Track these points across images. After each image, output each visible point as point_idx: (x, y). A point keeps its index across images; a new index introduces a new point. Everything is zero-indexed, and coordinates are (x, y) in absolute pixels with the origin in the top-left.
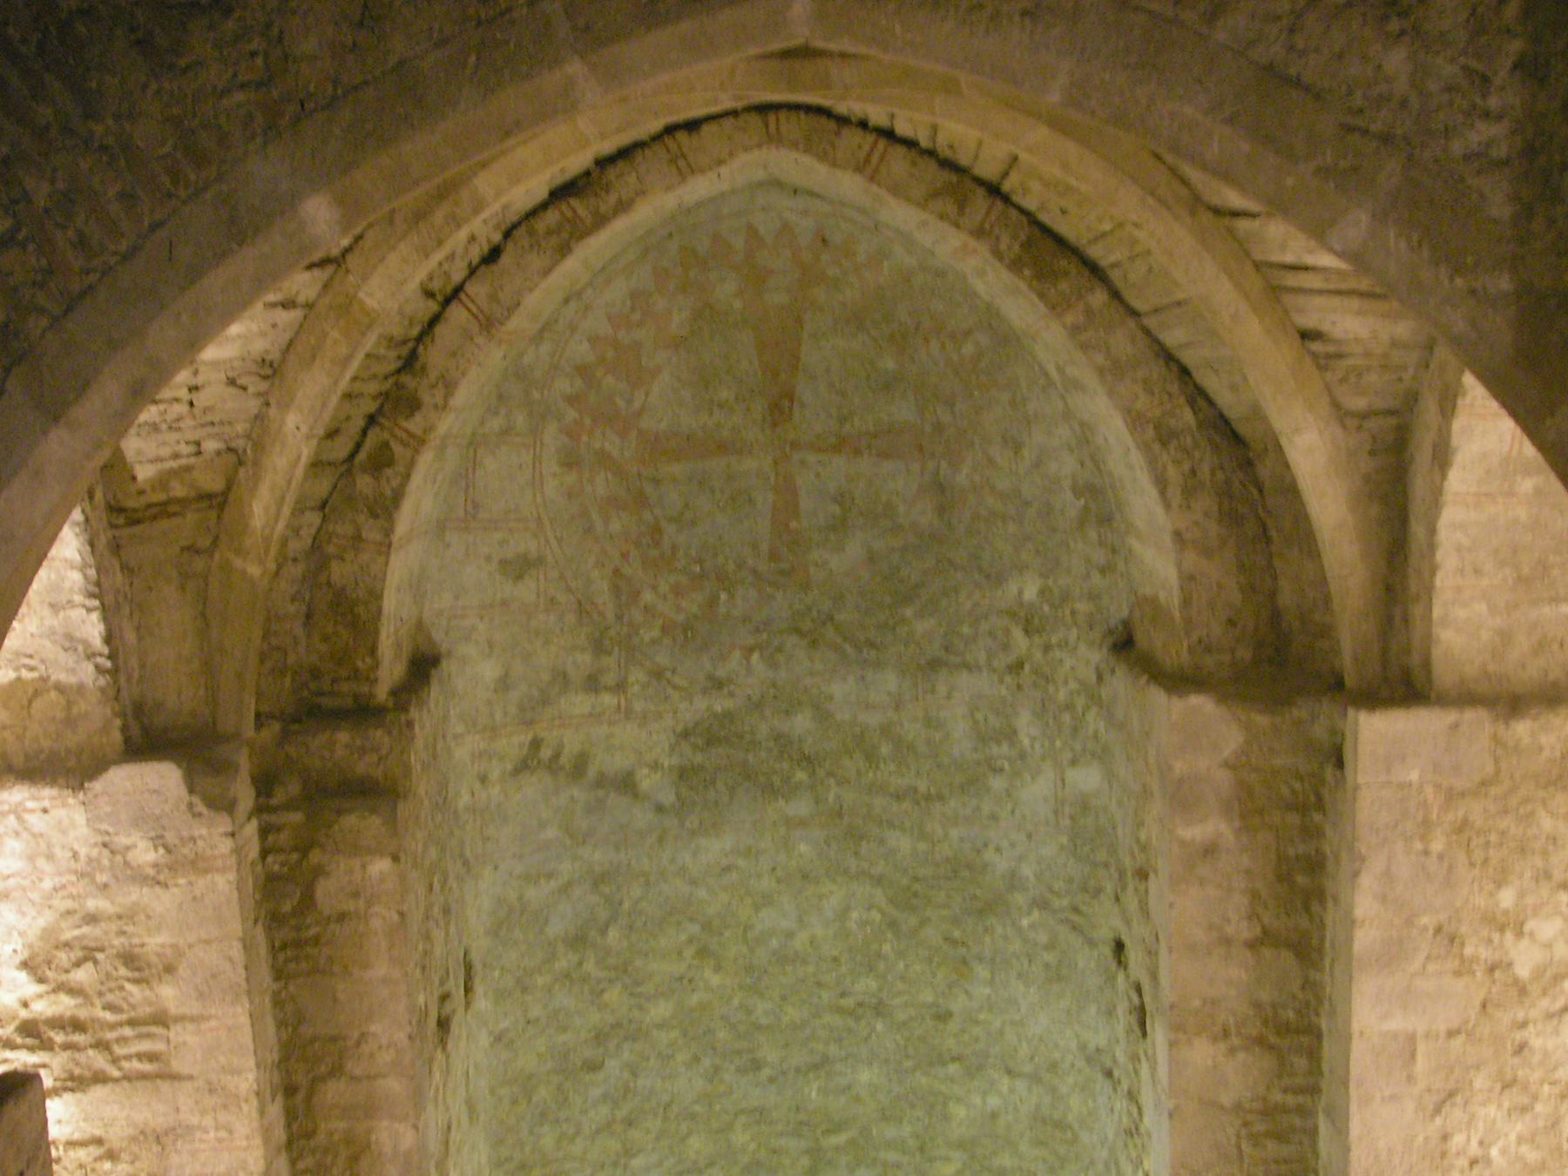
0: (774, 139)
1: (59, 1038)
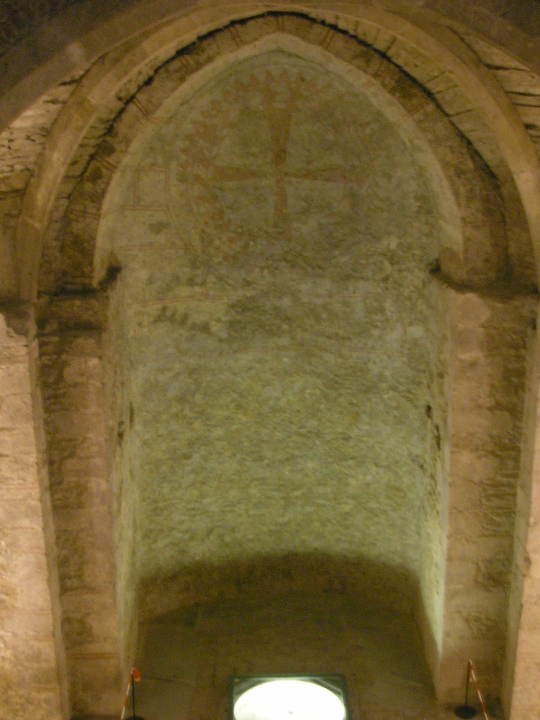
0: (282, 29)
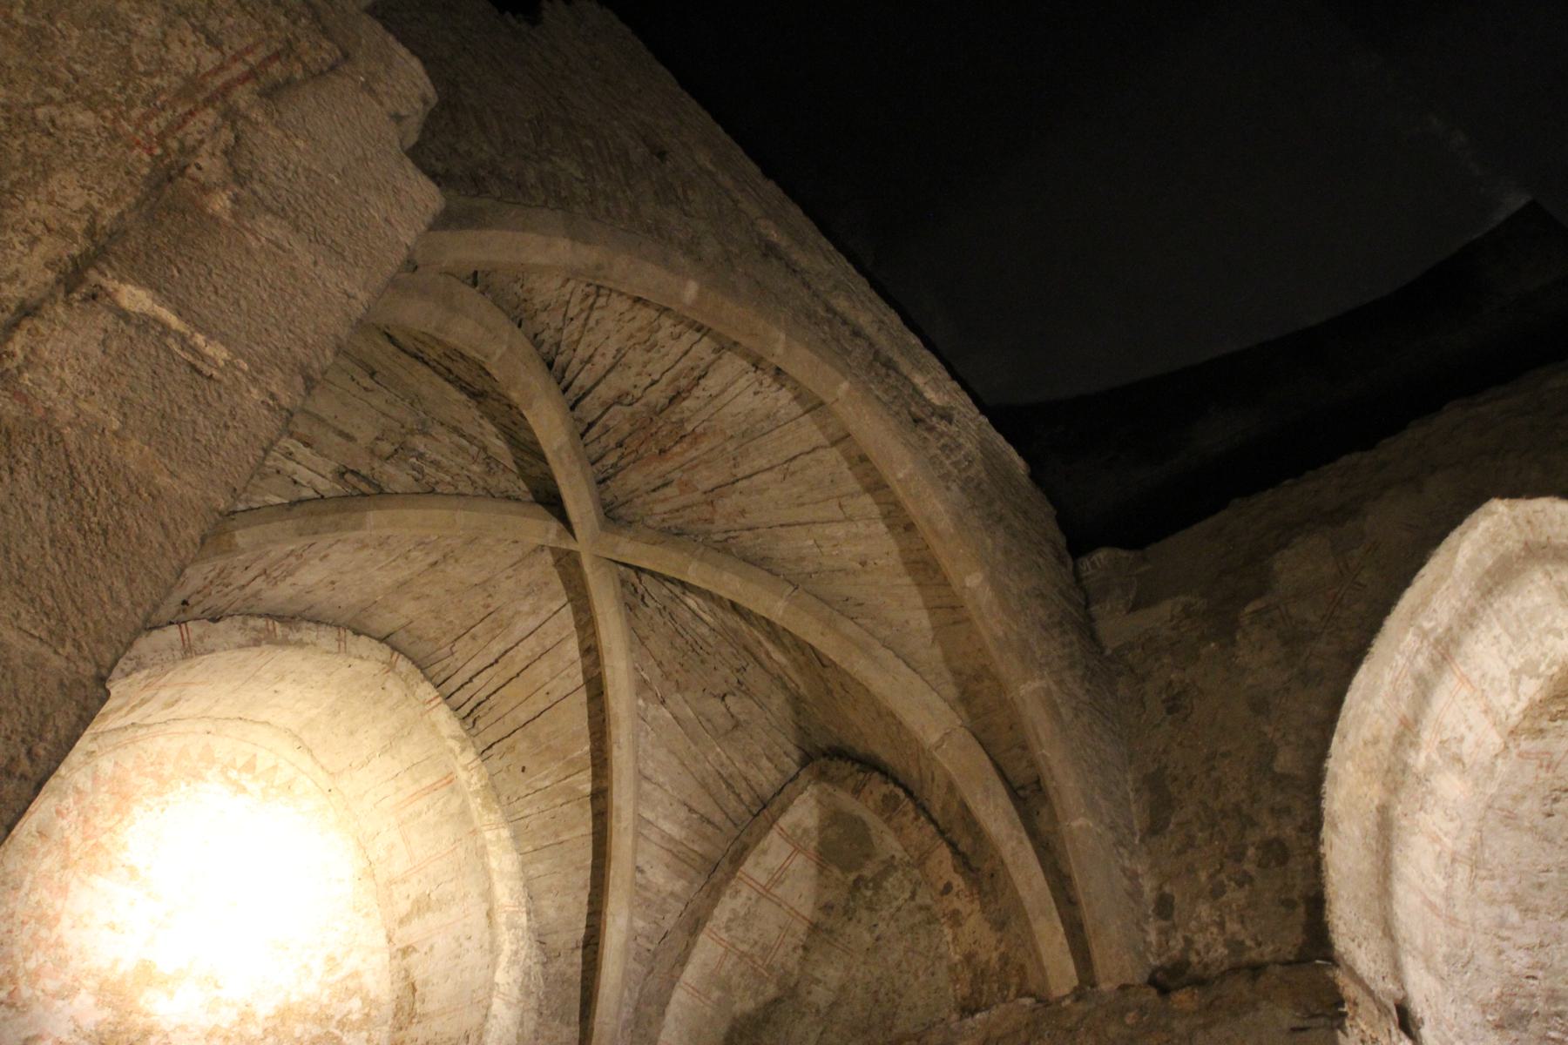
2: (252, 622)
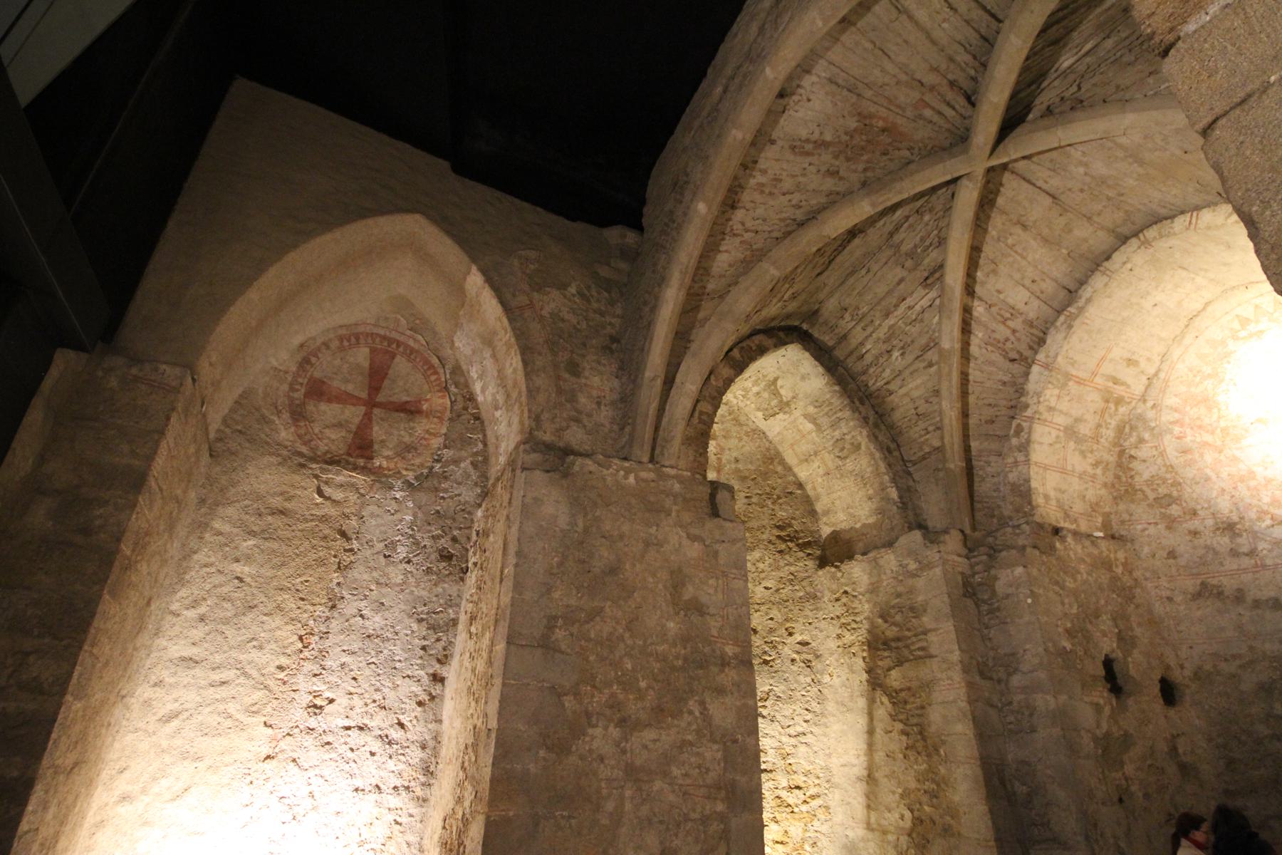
1: (893, 644)
2: (1058, 324)
